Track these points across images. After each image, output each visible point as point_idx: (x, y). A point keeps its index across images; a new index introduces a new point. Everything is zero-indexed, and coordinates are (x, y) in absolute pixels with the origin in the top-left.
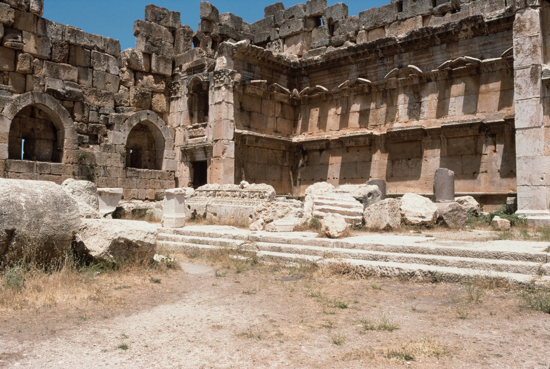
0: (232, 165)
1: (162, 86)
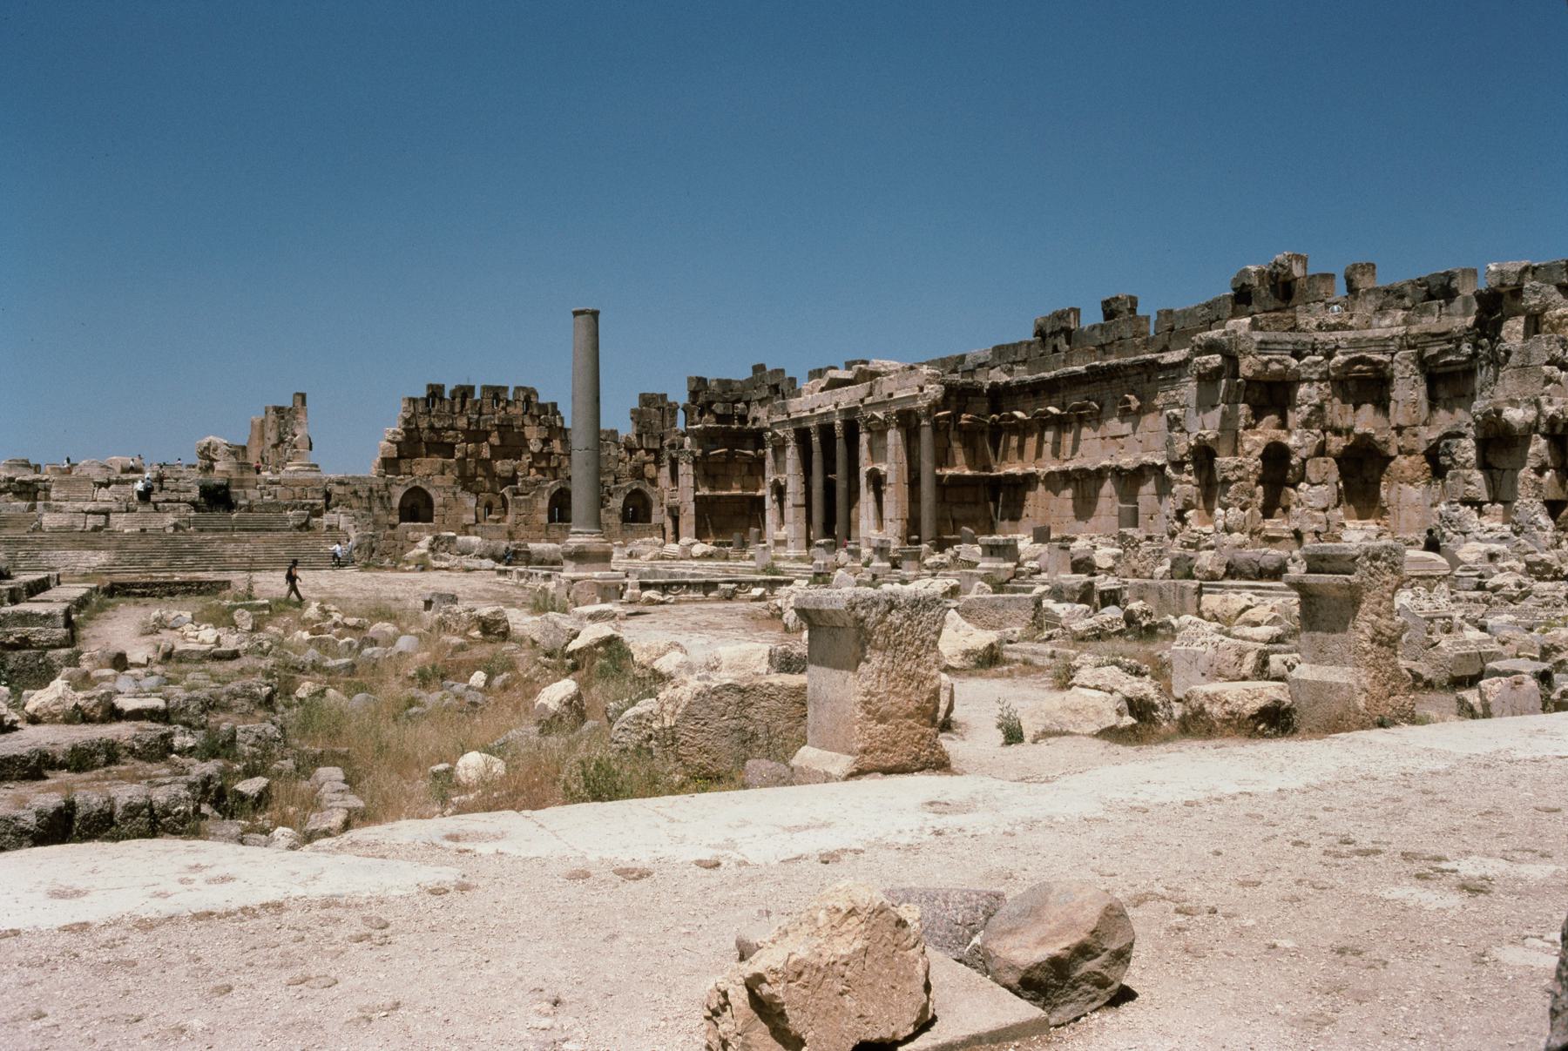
0: (693, 519)
1: (652, 457)
